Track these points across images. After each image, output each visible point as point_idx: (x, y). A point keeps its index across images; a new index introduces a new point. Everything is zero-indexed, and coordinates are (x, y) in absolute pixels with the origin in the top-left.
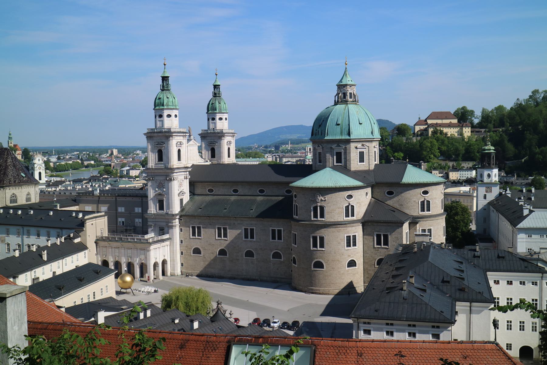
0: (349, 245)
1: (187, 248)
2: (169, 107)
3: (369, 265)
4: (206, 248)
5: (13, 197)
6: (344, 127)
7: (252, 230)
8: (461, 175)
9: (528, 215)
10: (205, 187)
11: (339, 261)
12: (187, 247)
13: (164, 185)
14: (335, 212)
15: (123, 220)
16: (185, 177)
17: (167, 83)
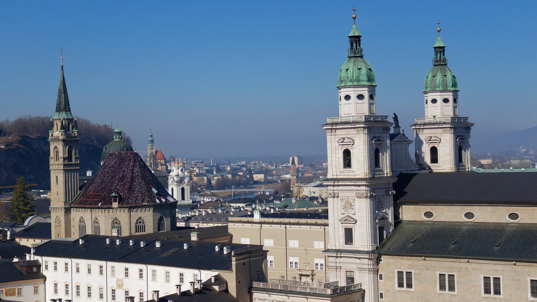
2: (361, 83)
5: (140, 222)
7: (496, 280)
13: (354, 206)
15: (296, 260)
16: (386, 191)
17: (358, 45)
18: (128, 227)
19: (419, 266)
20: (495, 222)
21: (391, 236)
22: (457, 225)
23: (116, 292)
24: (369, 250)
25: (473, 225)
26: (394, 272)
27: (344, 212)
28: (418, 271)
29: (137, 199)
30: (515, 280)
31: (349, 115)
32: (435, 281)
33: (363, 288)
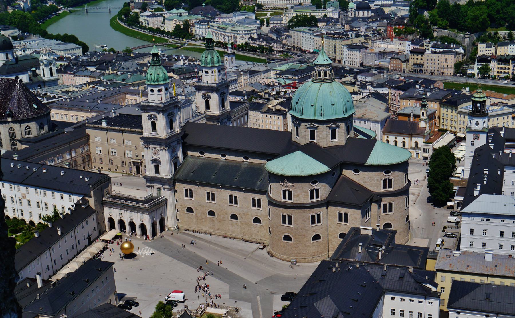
0: (313, 222)
5: (28, 129)
6: (317, 109)
8: (511, 50)
9: (477, 196)
11: (304, 235)
12: (181, 206)
18: (20, 133)
21: (181, 166)
22: (217, 161)
23: (23, 200)
25: (225, 161)
27: (154, 156)
28: (195, 190)
29: (24, 114)
31: (153, 102)
33: (166, 197)
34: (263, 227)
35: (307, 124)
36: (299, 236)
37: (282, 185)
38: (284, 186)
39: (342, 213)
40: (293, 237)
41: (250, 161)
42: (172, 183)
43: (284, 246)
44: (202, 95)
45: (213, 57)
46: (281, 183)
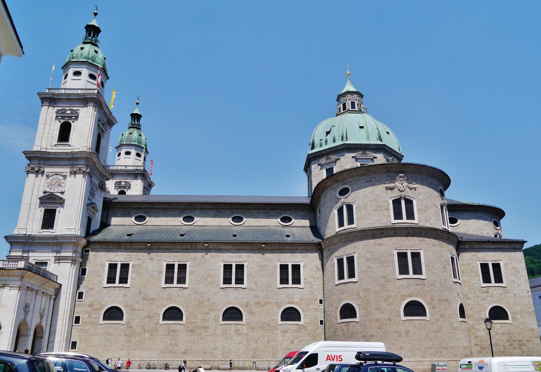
1: (90, 309)
3: (476, 320)
4: (136, 307)
6: (370, 131)
10: (129, 212)
11: (447, 301)
13: (63, 183)
14: (430, 211)
19: (140, 256)
20: (217, 225)
24: (77, 234)
26: (105, 264)
27: (48, 190)
28: (137, 262)
30: (261, 266)
32: (161, 272)
34: (305, 328)
35: (354, 155)
36: (440, 300)
37: (392, 189)
38: (396, 190)
39: (488, 264)
40: (429, 304)
41: (244, 225)
42: (80, 250)
43: (407, 332)
44: (115, 184)
45: (140, 135)
46: (387, 185)
